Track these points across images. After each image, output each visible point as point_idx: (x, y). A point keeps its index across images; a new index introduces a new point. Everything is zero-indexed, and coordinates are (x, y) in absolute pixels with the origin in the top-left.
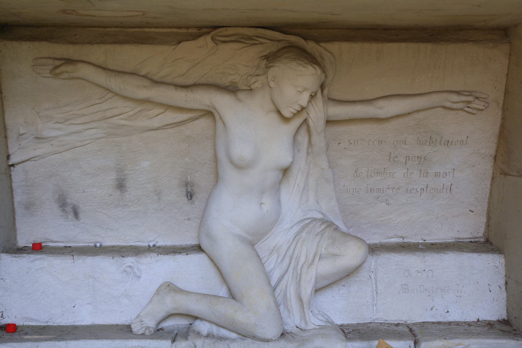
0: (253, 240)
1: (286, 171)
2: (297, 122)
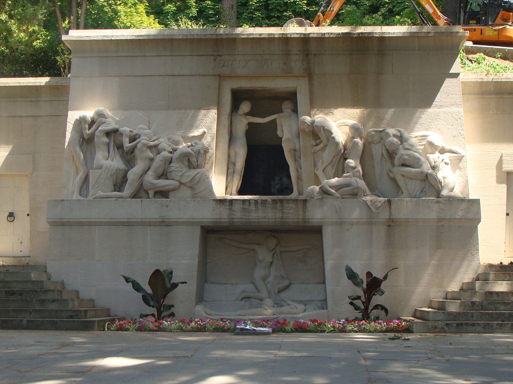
0: (264, 279)
1: (271, 263)
2: (273, 252)
